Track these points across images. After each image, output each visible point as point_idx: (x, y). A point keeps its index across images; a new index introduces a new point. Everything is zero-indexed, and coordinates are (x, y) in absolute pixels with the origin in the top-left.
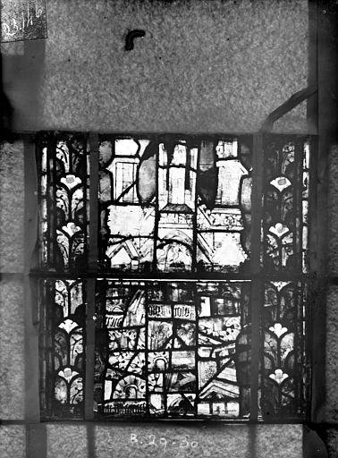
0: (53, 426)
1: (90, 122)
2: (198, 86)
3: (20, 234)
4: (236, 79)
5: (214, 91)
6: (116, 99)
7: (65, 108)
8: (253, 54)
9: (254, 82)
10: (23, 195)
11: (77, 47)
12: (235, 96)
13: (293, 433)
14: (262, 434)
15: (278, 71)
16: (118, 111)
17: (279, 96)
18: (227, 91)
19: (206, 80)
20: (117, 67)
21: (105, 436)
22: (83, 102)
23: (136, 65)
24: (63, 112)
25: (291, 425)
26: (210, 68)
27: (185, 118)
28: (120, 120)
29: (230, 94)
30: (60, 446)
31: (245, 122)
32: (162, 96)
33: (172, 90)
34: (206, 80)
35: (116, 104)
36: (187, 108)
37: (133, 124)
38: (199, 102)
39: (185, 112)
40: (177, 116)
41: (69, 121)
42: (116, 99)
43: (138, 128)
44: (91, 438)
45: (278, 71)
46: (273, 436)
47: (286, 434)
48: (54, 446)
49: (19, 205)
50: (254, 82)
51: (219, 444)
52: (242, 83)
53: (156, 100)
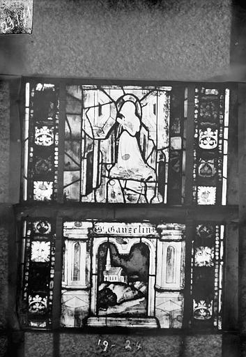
0: (30, 334)
1: (54, 69)
2: (138, 44)
3: (6, 173)
4: (166, 40)
5: (149, 48)
6: (74, 50)
7: (34, 57)
8: (180, 20)
9: (181, 41)
10: (8, 142)
11: (45, 10)
12: (166, 52)
13: (215, 342)
14: (192, 343)
15: (199, 33)
16: (76, 60)
17: (199, 52)
18: (160, 48)
19: (144, 40)
20: (75, 26)
21: (70, 342)
22: (49, 53)
23: (90, 26)
24: (33, 61)
25: (213, 336)
26: (147, 32)
27: (127, 68)
28: (77, 68)
29: (162, 51)
30: (35, 350)
31: (174, 71)
32: (110, 51)
33: (117, 46)
34: (144, 40)
35: (74, 55)
36: (129, 60)
37: (87, 72)
38: (138, 56)
39: (127, 63)
40: (121, 66)
41: (37, 68)
42: (74, 50)
43: (90, 75)
44: (56, 344)
45: (199, 33)
46: (200, 345)
47: (210, 342)
48: (30, 349)
49: (5, 150)
50: (181, 41)
51: (158, 350)
52: (171, 42)
53: (104, 54)
